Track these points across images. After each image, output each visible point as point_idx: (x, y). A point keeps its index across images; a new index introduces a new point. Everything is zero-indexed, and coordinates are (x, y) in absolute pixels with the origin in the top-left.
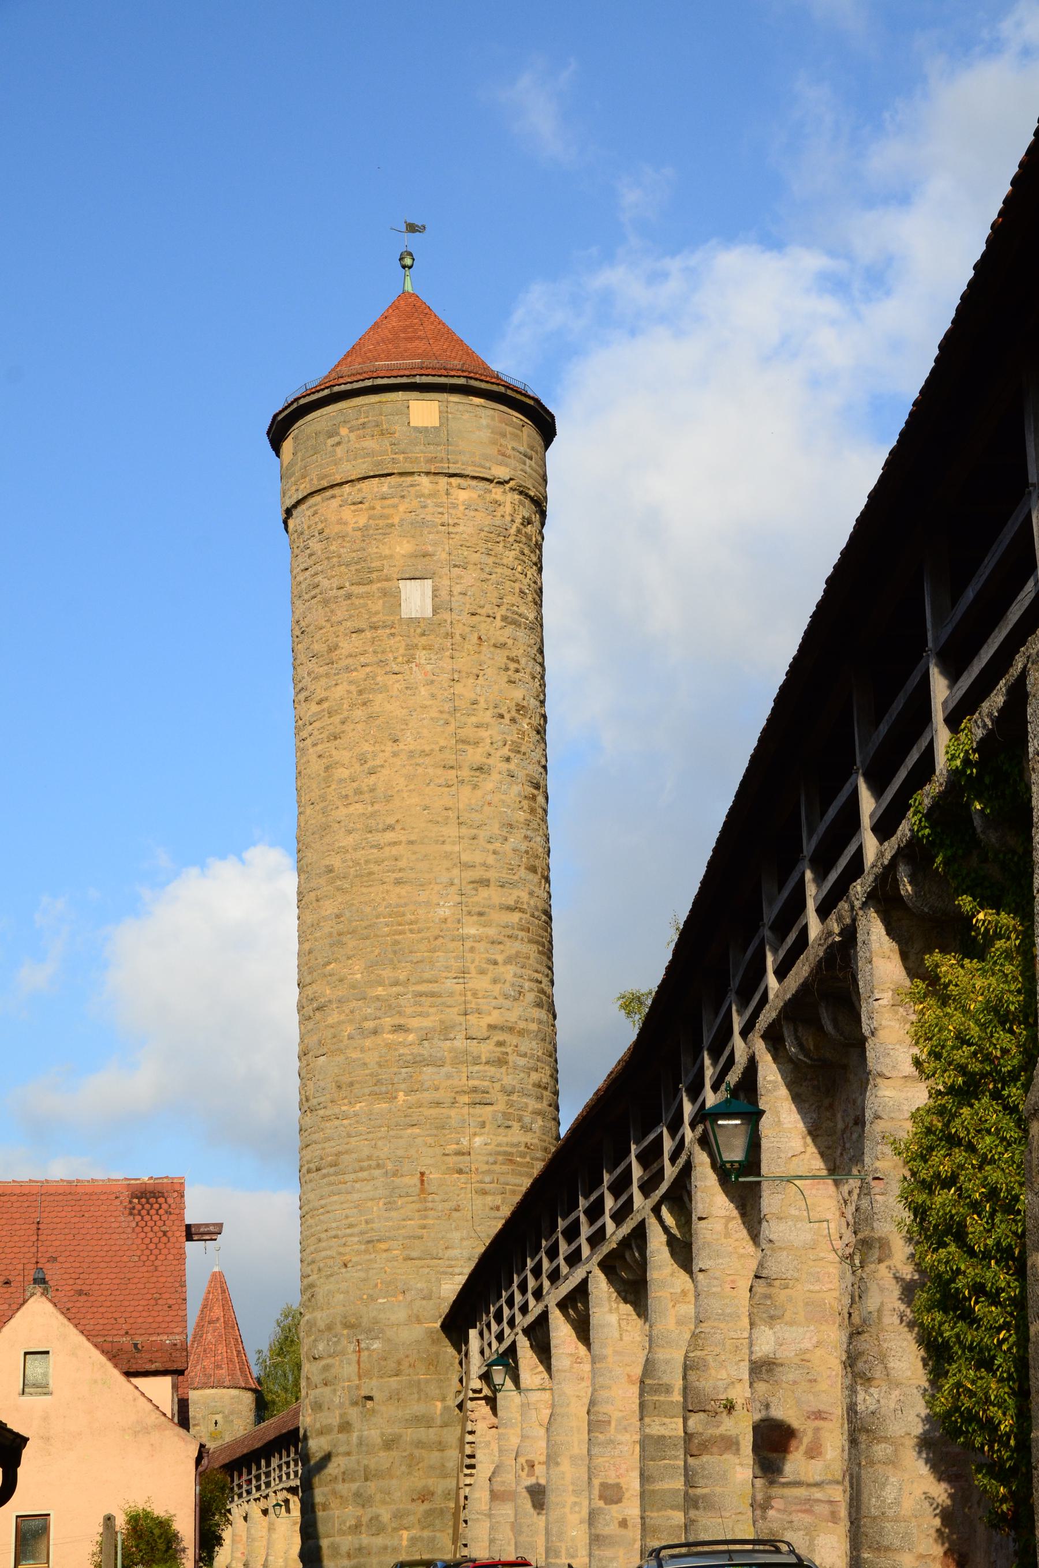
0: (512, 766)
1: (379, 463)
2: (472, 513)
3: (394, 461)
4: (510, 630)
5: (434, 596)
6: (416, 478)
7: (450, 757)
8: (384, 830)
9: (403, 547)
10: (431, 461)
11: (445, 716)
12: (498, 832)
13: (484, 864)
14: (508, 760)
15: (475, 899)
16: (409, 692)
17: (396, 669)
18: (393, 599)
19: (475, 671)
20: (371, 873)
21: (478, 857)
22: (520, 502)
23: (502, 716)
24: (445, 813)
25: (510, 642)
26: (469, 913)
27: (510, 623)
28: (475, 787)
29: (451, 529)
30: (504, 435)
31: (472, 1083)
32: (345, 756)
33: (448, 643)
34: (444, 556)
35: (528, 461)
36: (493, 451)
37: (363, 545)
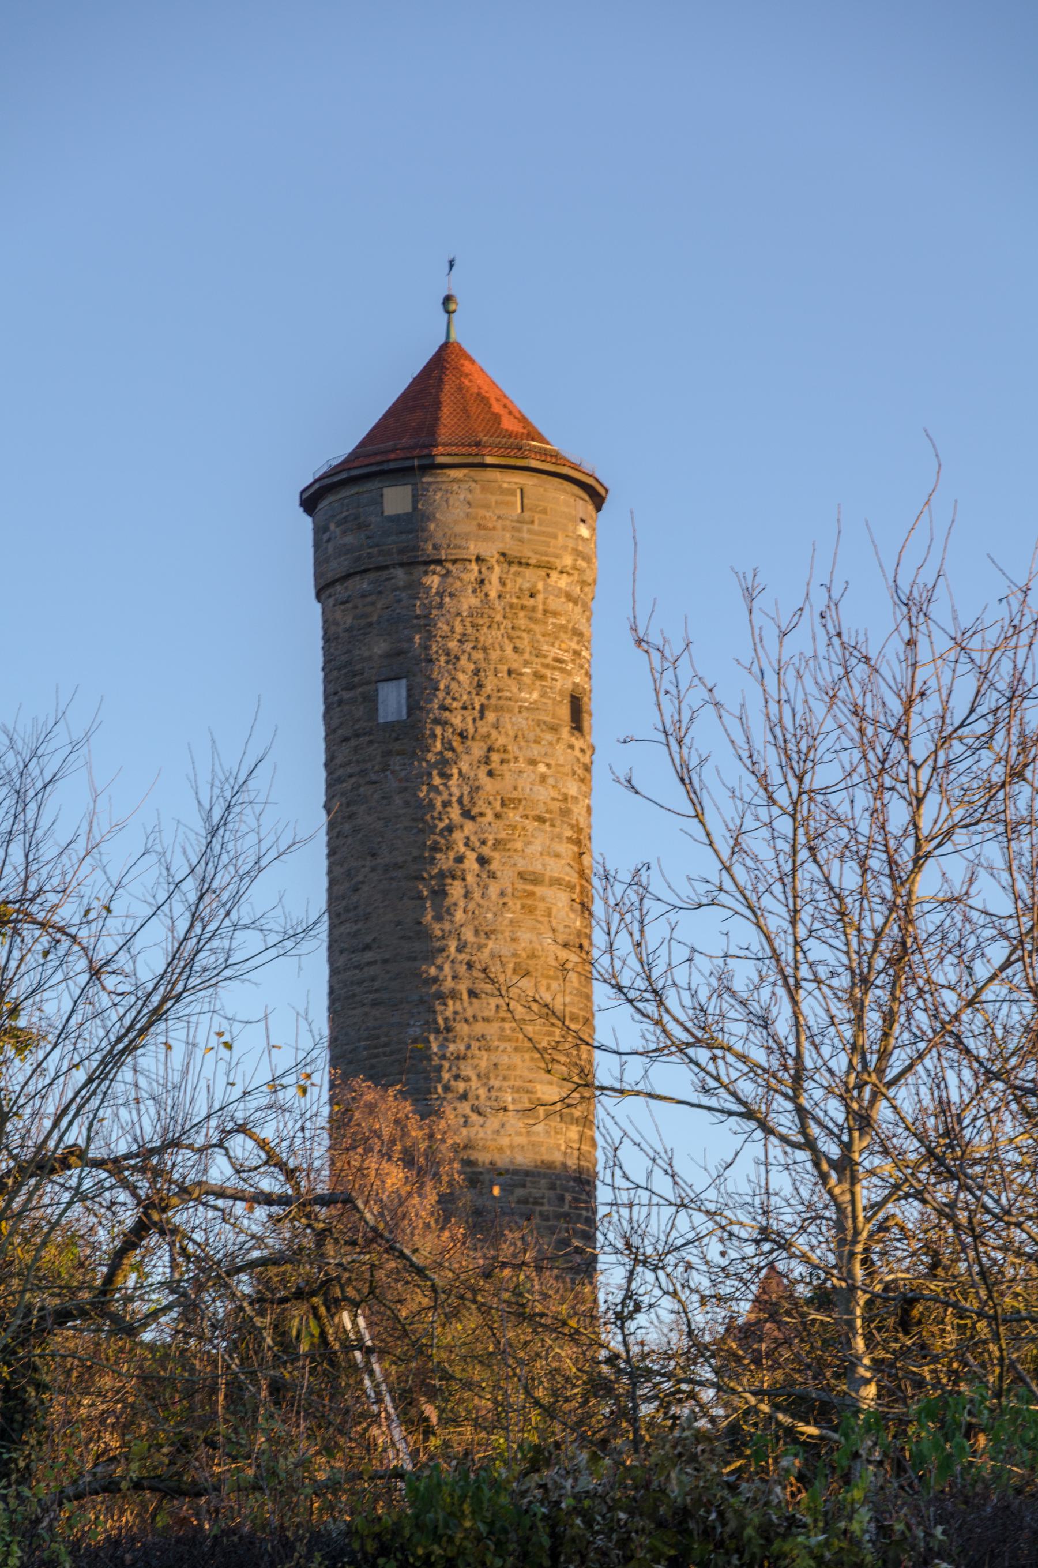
0: (494, 866)
3: (370, 556)
5: (409, 696)
9: (380, 647)
10: (401, 552)
16: (385, 802)
17: (374, 777)
18: (371, 700)
20: (354, 995)
23: (482, 815)
35: (525, 527)
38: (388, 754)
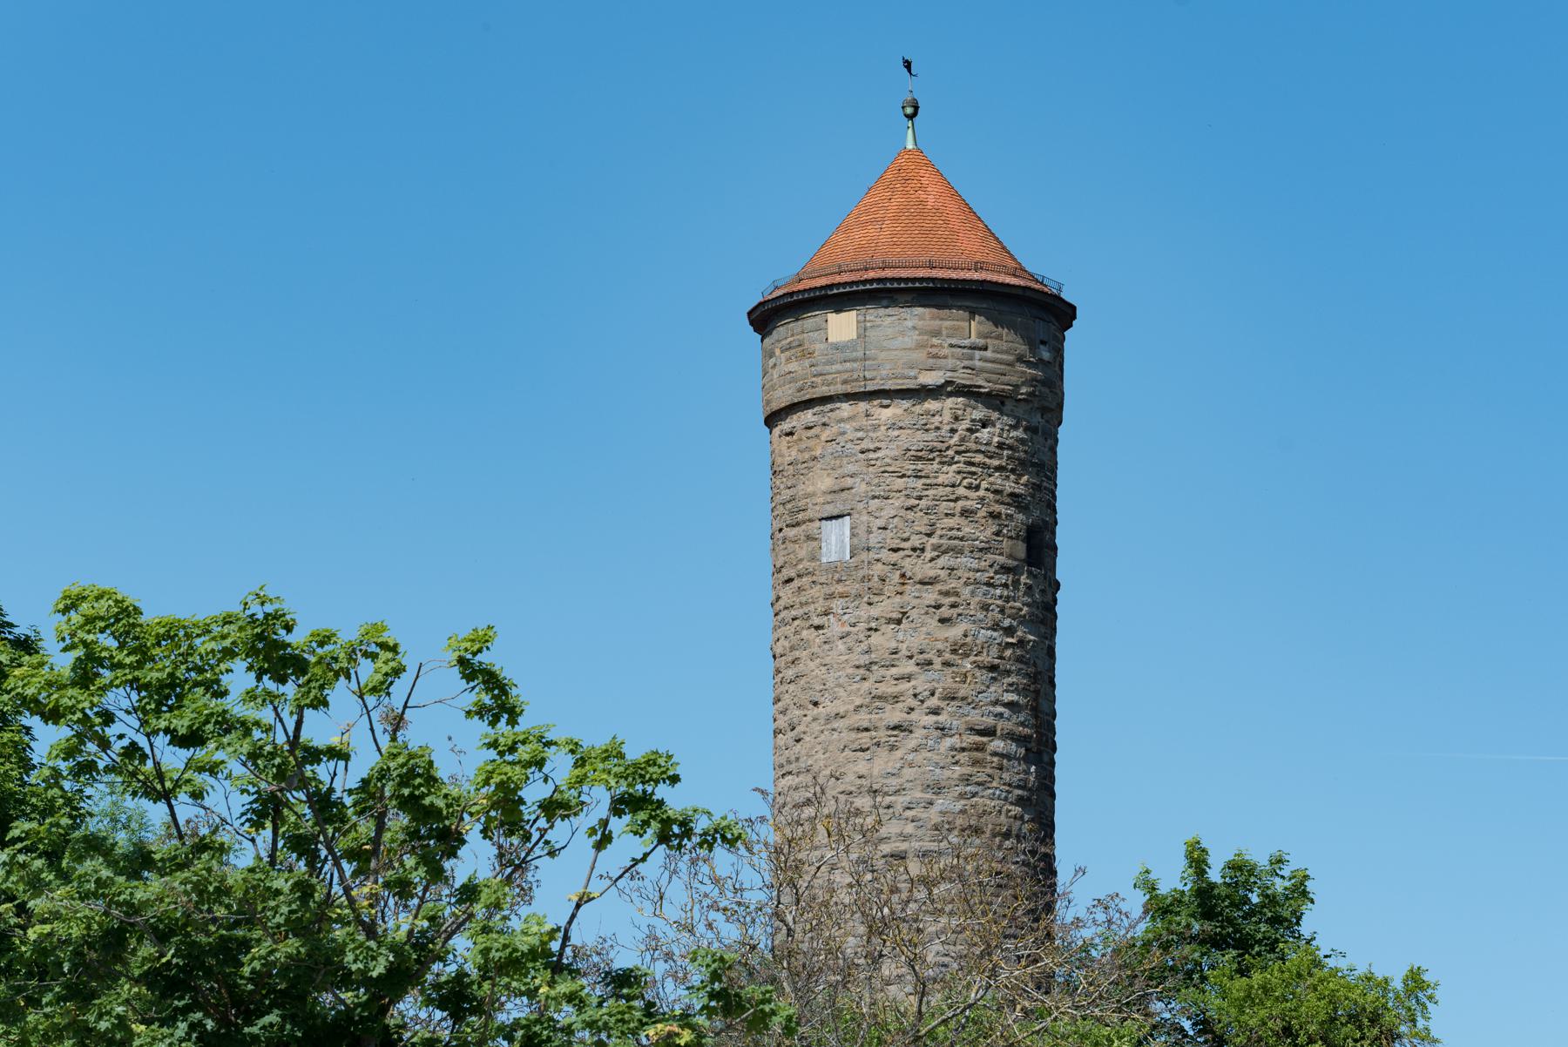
0: (941, 718)
2: (896, 433)
4: (944, 560)
5: (853, 535)
7: (863, 719)
9: (825, 482)
10: (845, 382)
11: (862, 671)
12: (919, 795)
14: (935, 712)
16: (827, 647)
17: (817, 621)
19: (895, 615)
24: (859, 782)
25: (943, 574)
27: (944, 552)
28: (893, 748)
29: (872, 455)
30: (936, 333)
34: (863, 487)
35: (978, 354)
36: (920, 356)
38: (830, 597)
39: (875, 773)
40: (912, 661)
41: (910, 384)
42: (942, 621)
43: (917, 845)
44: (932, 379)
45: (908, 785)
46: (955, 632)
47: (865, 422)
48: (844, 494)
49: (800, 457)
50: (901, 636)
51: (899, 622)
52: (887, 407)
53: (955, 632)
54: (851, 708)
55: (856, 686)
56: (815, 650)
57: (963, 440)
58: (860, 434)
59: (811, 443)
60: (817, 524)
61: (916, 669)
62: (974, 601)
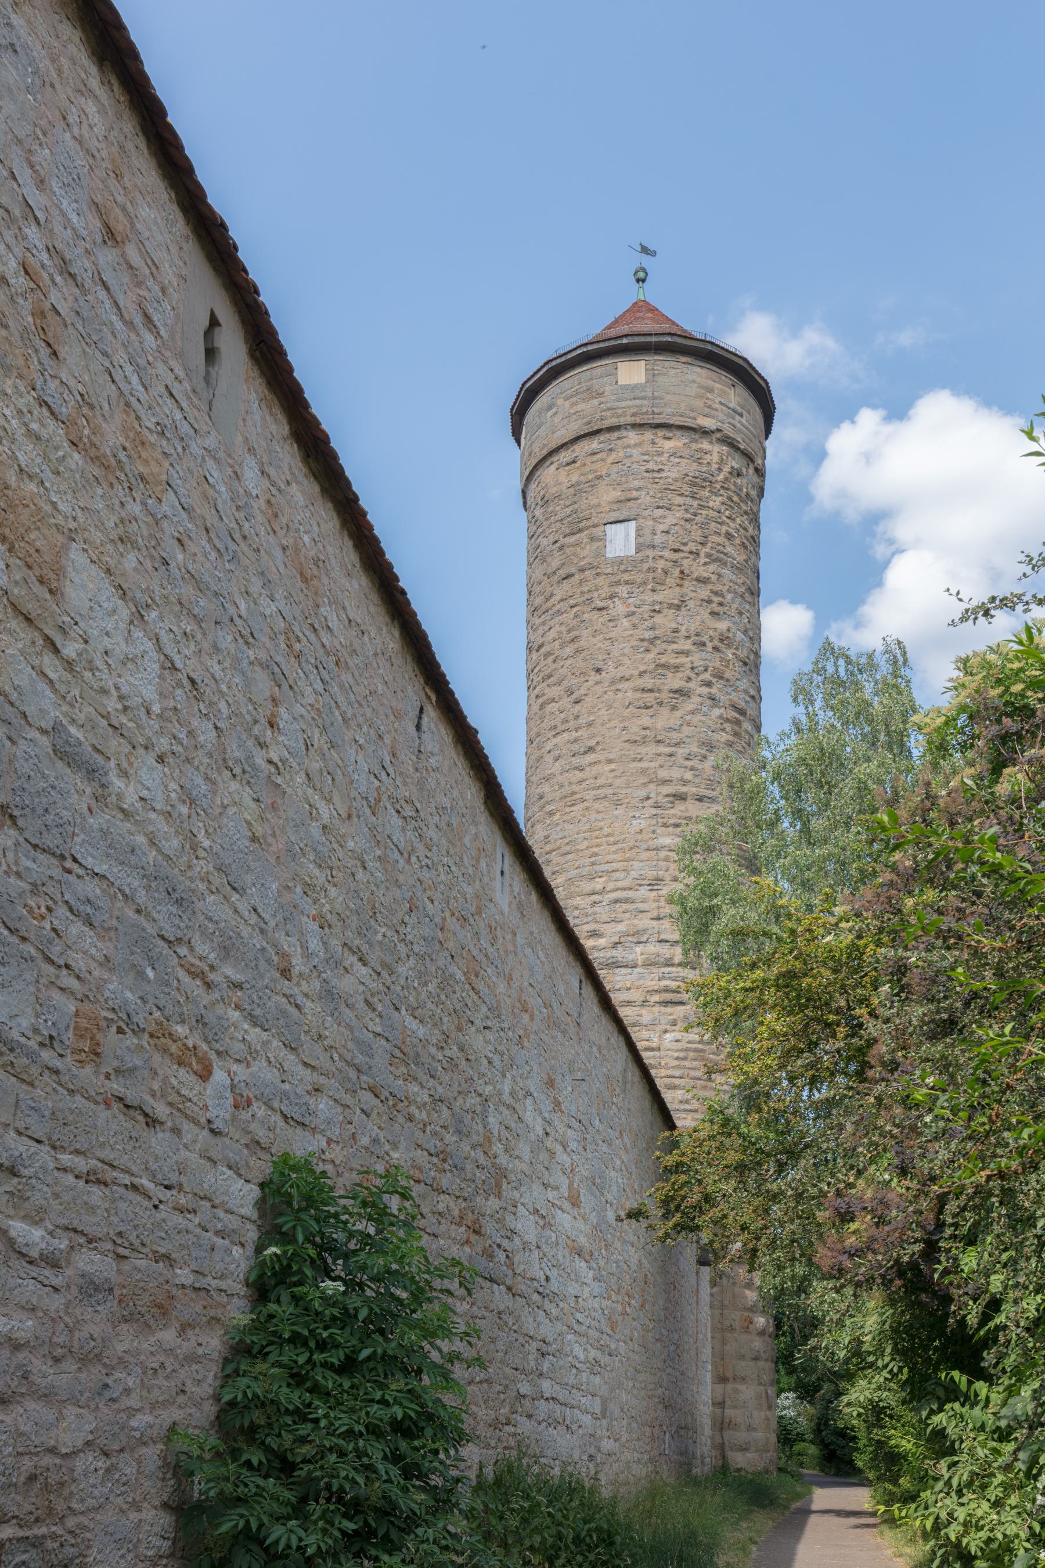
1: (589, 423)
4: (713, 567)
6: (624, 433)
7: (648, 682)
8: (585, 753)
10: (634, 415)
11: (645, 644)
12: (696, 750)
13: (682, 779)
14: (709, 684)
15: (672, 812)
16: (611, 624)
17: (600, 604)
20: (574, 793)
21: (675, 773)
22: (729, 454)
24: (644, 733)
25: (714, 577)
26: (665, 825)
28: (674, 708)
29: (656, 475)
30: (711, 390)
31: (663, 983)
32: (554, 692)
33: (651, 575)
34: (648, 499)
35: (737, 417)
36: (699, 403)
37: (575, 499)
38: (618, 583)
39: (659, 726)
40: (690, 641)
41: (689, 423)
42: (713, 613)
43: (694, 790)
44: (708, 423)
45: (687, 740)
46: (722, 625)
47: (650, 448)
48: (630, 504)
49: (583, 479)
50: (680, 619)
51: (678, 607)
52: (669, 439)
53: (722, 625)
54: (636, 672)
55: (639, 656)
56: (599, 626)
57: (726, 479)
58: (646, 457)
59: (594, 467)
60: (602, 528)
61: (693, 648)
62: (735, 606)
